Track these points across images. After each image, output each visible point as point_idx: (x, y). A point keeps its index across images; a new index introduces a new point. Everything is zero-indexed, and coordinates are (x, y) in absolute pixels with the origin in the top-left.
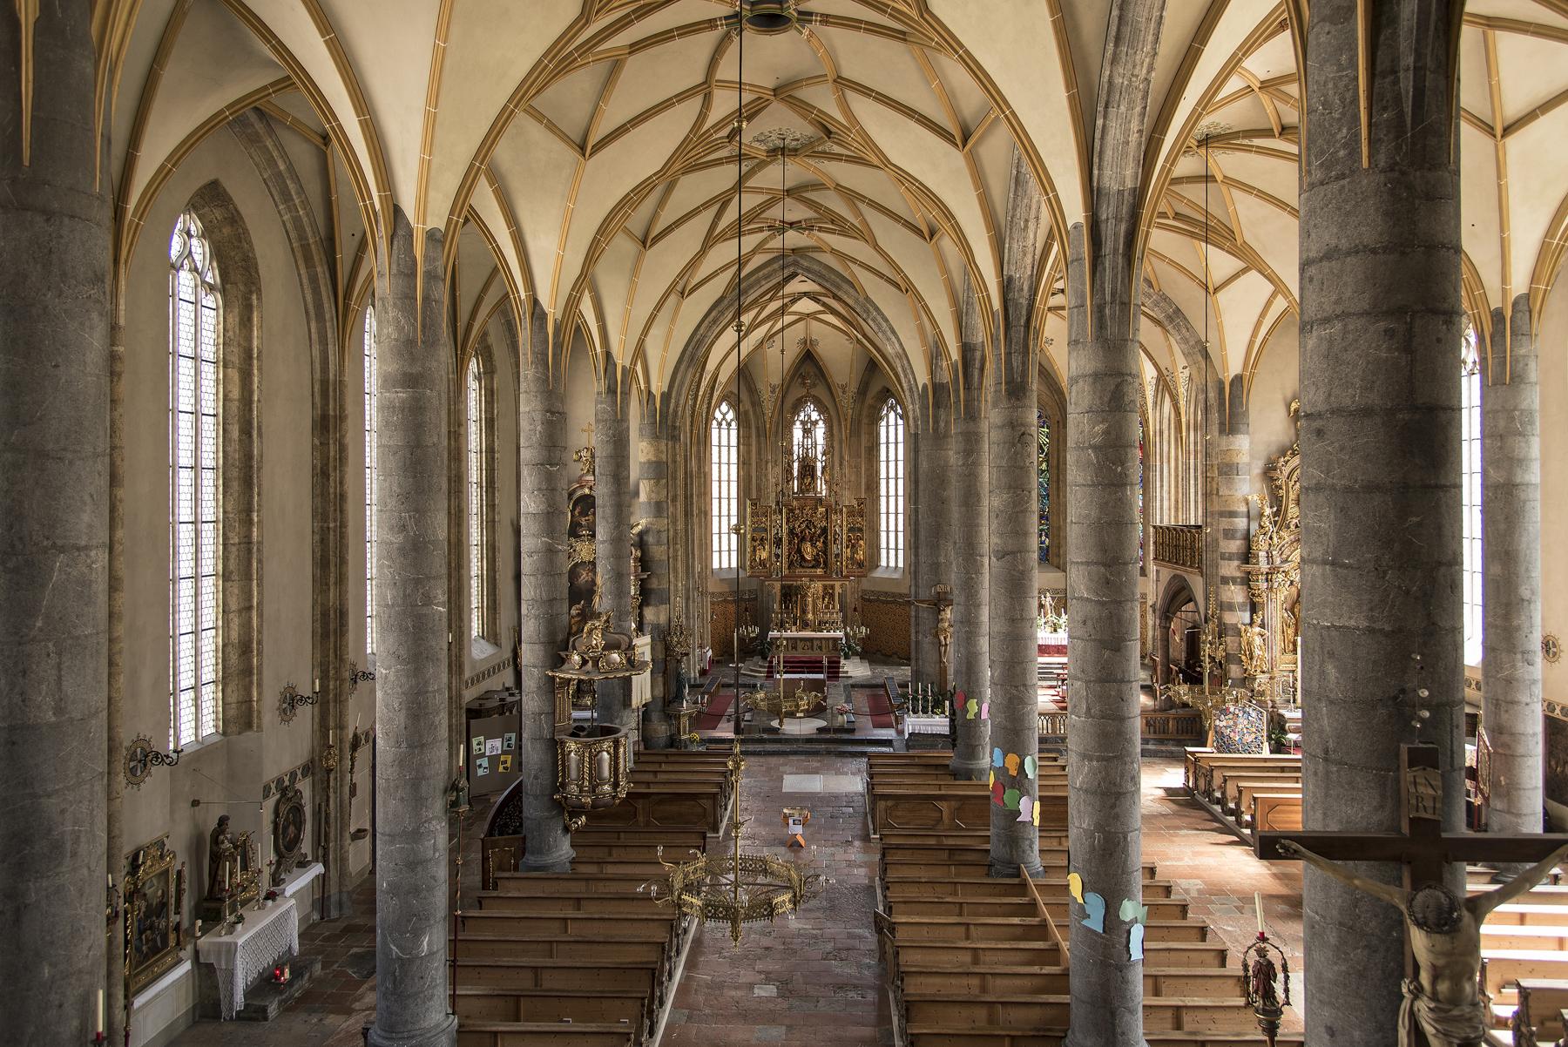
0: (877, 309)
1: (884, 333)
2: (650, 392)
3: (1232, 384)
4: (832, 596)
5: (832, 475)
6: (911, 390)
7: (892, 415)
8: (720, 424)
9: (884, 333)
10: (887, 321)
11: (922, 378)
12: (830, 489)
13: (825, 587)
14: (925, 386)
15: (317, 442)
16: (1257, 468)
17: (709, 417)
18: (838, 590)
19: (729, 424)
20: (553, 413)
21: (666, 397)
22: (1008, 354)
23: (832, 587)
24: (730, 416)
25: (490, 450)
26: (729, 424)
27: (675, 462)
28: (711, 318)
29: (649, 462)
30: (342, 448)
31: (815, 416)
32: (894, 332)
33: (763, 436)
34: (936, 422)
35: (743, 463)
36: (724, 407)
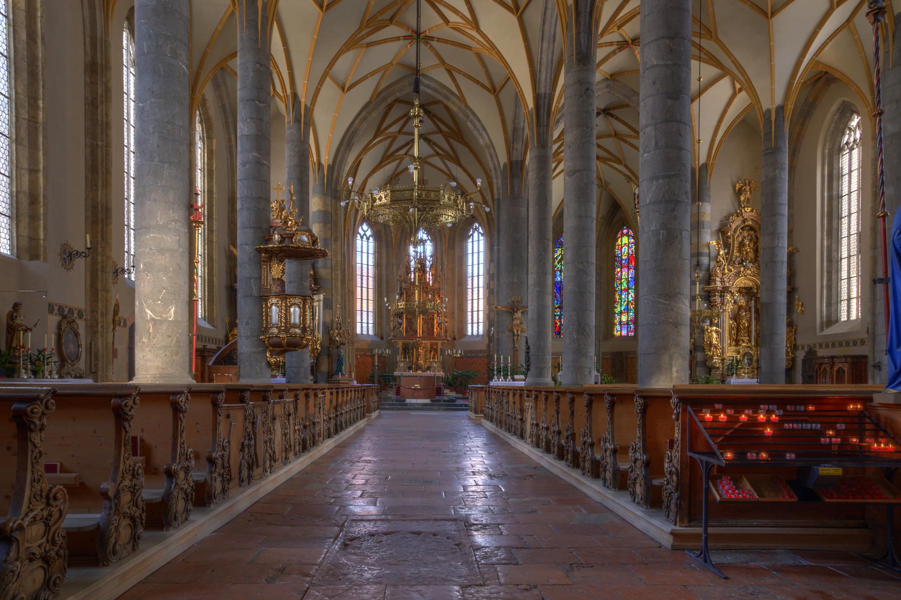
0: (473, 113)
1: (478, 130)
2: (320, 164)
3: (700, 169)
4: (436, 351)
5: (436, 270)
6: (495, 169)
7: (476, 234)
8: (362, 237)
9: (478, 130)
10: (479, 121)
11: (503, 159)
12: (434, 281)
13: (432, 345)
14: (505, 165)
15: (88, 80)
16: (716, 225)
17: (355, 232)
18: (440, 346)
19: (368, 239)
20: (261, 65)
21: (331, 168)
22: (578, 34)
23: (436, 344)
24: (369, 233)
25: (210, 192)
26: (368, 239)
27: (337, 214)
28: (361, 116)
29: (319, 211)
30: (107, 90)
31: (425, 237)
32: (484, 129)
33: (391, 244)
34: (512, 188)
35: (378, 265)
36: (365, 227)
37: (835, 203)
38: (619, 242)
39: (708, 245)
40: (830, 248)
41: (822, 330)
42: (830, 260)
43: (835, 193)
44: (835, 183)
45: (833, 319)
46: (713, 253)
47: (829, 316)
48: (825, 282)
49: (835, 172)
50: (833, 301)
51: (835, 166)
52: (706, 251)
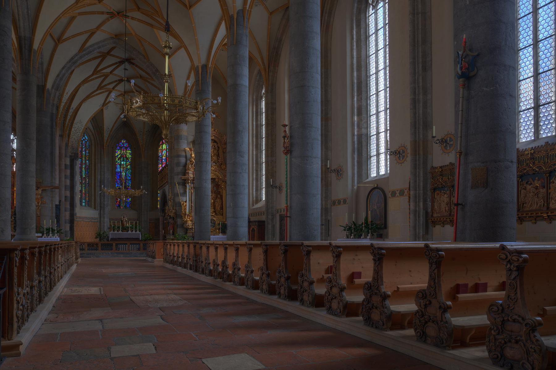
37: (259, 129)
38: (161, 148)
39: (185, 151)
40: (257, 155)
41: (253, 205)
42: (257, 163)
43: (259, 123)
44: (259, 117)
45: (259, 199)
46: (188, 156)
47: (257, 197)
48: (254, 176)
49: (259, 110)
50: (259, 188)
51: (259, 107)
52: (184, 154)
